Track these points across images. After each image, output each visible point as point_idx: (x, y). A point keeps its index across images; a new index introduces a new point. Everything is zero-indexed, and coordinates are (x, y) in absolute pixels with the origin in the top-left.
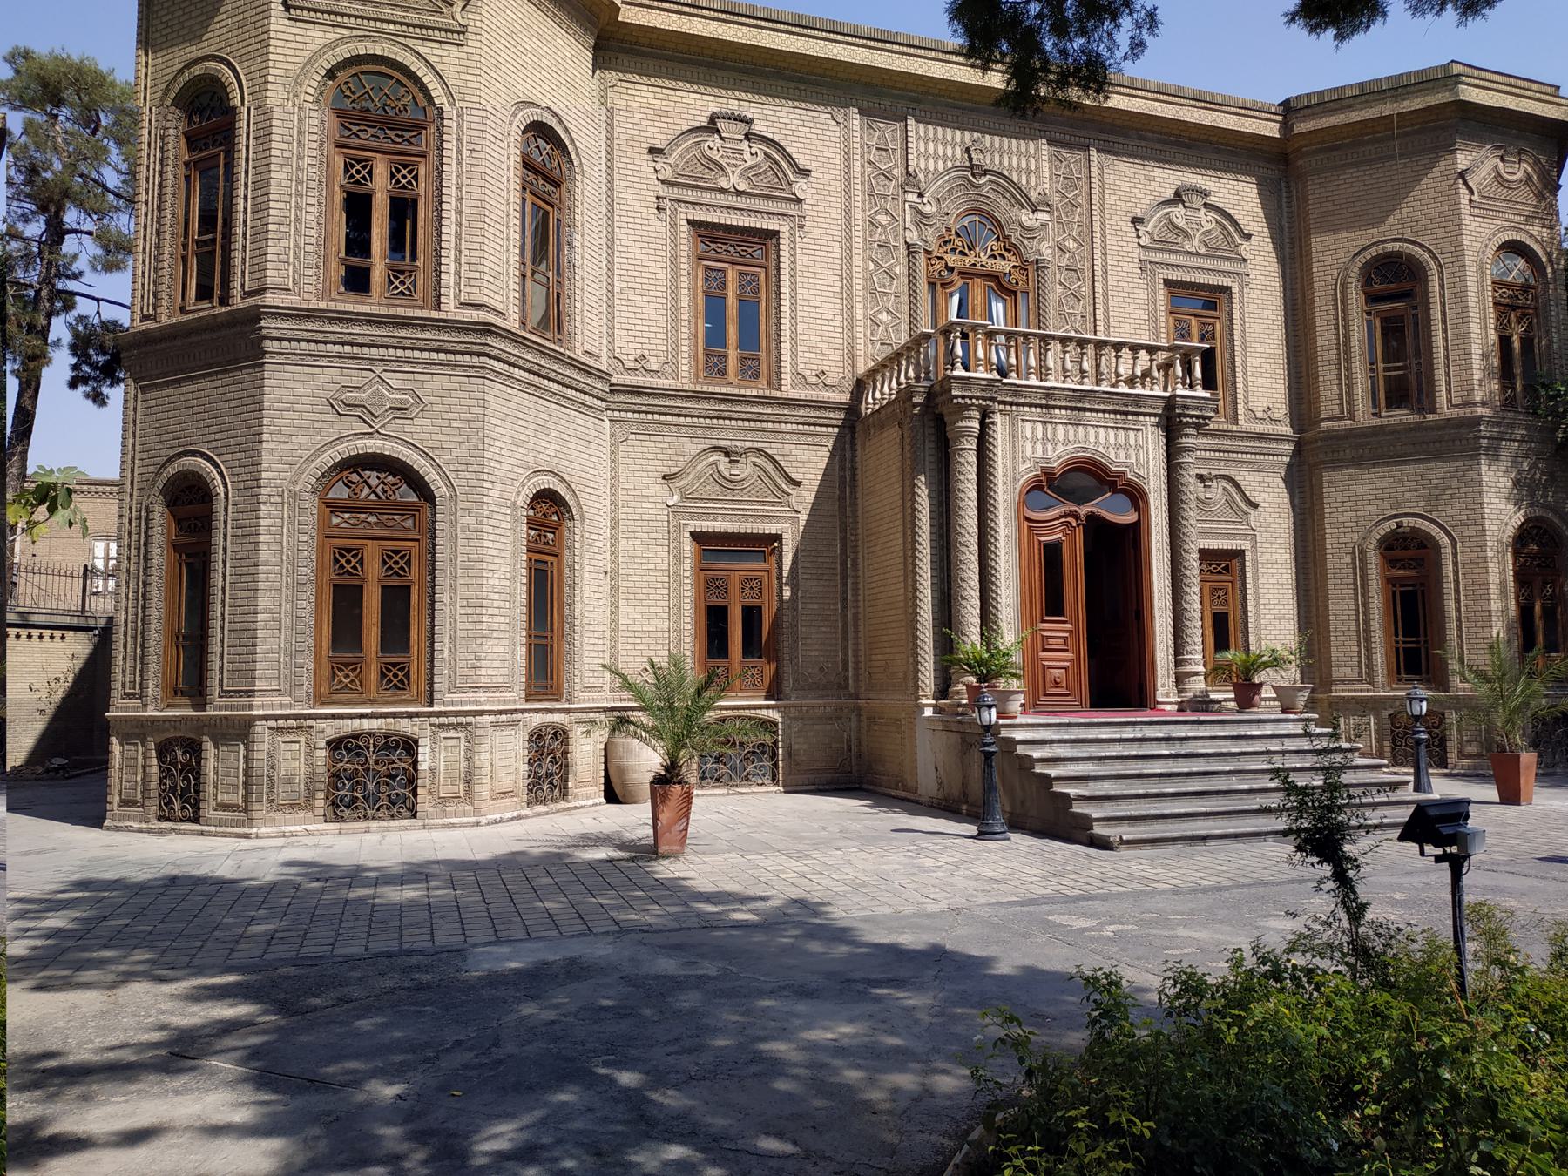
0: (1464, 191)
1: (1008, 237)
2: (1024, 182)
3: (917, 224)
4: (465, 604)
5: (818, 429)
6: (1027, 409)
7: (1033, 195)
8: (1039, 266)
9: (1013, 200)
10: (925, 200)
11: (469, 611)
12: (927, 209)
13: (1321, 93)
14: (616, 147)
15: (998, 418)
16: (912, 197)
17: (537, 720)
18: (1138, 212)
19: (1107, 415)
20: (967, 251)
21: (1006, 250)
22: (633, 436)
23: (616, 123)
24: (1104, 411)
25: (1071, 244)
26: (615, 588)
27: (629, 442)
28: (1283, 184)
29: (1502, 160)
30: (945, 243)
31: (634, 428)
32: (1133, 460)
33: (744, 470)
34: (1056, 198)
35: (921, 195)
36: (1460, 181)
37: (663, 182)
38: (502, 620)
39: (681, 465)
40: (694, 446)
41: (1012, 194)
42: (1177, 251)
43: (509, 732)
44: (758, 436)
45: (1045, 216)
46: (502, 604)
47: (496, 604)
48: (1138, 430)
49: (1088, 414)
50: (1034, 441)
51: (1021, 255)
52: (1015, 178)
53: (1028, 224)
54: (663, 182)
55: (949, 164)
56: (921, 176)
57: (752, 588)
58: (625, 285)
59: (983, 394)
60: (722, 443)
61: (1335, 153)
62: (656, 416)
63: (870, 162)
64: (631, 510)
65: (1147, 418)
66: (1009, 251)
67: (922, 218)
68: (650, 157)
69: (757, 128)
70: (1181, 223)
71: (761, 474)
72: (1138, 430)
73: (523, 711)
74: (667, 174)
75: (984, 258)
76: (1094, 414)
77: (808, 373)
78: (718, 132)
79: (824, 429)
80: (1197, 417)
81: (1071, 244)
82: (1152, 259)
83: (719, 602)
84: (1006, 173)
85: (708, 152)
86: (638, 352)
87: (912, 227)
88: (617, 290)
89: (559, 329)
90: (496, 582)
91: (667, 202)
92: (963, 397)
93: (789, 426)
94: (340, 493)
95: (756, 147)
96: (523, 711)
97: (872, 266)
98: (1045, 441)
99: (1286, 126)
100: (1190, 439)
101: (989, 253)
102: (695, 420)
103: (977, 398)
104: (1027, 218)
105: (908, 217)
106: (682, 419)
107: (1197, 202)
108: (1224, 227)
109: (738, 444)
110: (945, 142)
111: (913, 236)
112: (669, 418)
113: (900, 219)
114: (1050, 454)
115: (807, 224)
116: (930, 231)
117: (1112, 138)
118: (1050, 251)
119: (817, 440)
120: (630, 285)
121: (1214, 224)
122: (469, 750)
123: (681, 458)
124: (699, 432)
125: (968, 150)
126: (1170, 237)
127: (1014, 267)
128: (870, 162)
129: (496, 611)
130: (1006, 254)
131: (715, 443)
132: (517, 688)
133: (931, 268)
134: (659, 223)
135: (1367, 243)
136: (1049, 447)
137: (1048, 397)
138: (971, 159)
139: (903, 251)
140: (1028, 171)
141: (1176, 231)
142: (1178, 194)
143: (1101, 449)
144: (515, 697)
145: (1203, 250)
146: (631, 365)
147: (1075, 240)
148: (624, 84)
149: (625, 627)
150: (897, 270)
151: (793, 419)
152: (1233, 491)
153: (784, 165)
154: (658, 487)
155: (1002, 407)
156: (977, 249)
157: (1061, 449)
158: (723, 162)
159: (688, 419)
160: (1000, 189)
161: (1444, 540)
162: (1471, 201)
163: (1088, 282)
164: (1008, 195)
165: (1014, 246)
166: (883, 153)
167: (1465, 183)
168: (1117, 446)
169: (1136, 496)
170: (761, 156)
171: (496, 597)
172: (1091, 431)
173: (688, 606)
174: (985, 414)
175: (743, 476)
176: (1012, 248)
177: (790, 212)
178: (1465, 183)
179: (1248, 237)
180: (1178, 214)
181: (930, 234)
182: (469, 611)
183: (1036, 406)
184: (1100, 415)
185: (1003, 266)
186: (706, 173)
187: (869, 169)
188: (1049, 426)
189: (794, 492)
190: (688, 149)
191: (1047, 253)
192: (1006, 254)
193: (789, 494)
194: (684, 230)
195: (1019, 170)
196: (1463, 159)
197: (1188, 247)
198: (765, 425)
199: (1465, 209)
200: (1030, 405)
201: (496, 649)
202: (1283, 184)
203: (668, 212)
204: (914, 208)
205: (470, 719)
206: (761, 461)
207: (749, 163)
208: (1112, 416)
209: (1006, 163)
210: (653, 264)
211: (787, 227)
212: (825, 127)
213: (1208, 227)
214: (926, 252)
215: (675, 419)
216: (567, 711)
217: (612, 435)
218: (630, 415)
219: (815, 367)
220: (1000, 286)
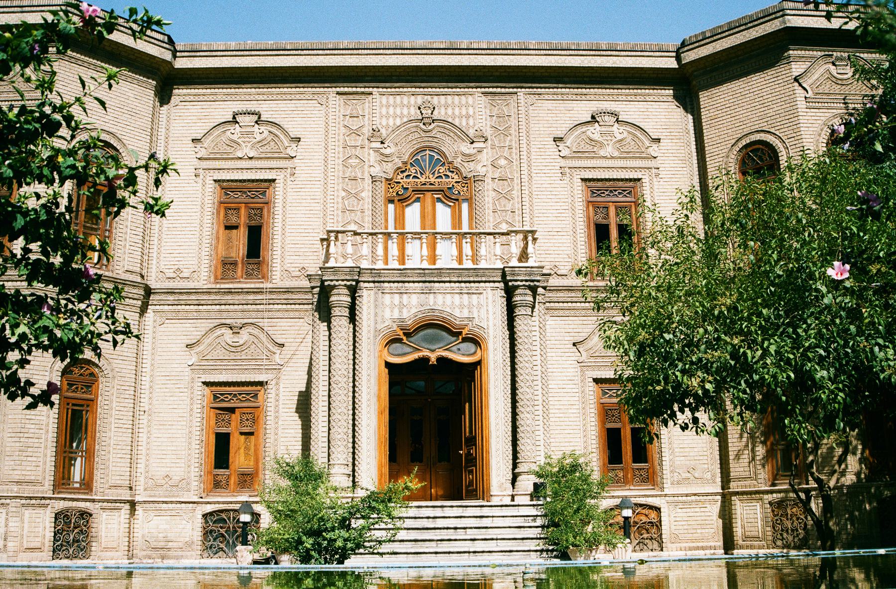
0: (800, 91)
1: (451, 163)
2: (464, 123)
3: (380, 162)
4: (10, 430)
5: (297, 306)
6: (386, 285)
7: (471, 133)
8: (477, 179)
9: (456, 138)
10: (385, 146)
11: (13, 435)
12: (387, 151)
13: (704, 33)
14: (170, 142)
15: (365, 293)
16: (378, 145)
17: (62, 505)
18: (560, 134)
19: (453, 284)
20: (419, 176)
21: (451, 171)
22: (167, 321)
23: (172, 128)
24: (450, 282)
25: (502, 162)
27: (165, 325)
28: (688, 100)
29: (834, 64)
30: (402, 172)
31: (169, 315)
32: (475, 315)
33: (244, 336)
34: (488, 132)
35: (382, 143)
36: (796, 84)
37: (199, 159)
38: (37, 440)
39: (198, 337)
40: (208, 325)
41: (454, 133)
42: (593, 158)
43: (41, 511)
44: (254, 314)
45: (481, 145)
46: (37, 431)
47: (32, 431)
48: (481, 293)
49: (437, 285)
50: (392, 307)
51: (461, 174)
52: (457, 122)
53: (467, 152)
54: (199, 159)
55: (405, 120)
56: (383, 131)
57: (247, 420)
58: (171, 226)
59: (348, 278)
60: (228, 321)
61: (714, 74)
62: (183, 307)
63: (345, 126)
64: (163, 370)
65: (487, 284)
66: (453, 172)
67: (385, 158)
68: (192, 145)
70: (596, 137)
71: (256, 341)
72: (481, 293)
73: (50, 498)
74: (203, 153)
75: (432, 180)
76: (442, 284)
77: (293, 269)
78: (237, 122)
79: (301, 306)
80: (526, 281)
81: (502, 162)
82: (571, 166)
83: (224, 430)
84: (450, 120)
85: (232, 137)
86: (176, 267)
87: (376, 165)
88: (165, 229)
90: (33, 417)
91: (201, 171)
92: (332, 280)
93: (276, 306)
95: (263, 128)
96: (50, 498)
97: (344, 194)
98: (402, 306)
99: (678, 58)
100: (522, 297)
101: (436, 175)
102: (209, 307)
103: (343, 280)
104: (466, 148)
105: (372, 159)
106: (200, 307)
107: (611, 120)
108: (634, 135)
109: (239, 321)
111: (376, 171)
112: (192, 307)
113: (366, 161)
114: (405, 315)
115: (296, 172)
116: (390, 164)
117: (534, 85)
118: (484, 169)
119: (297, 314)
120: (174, 225)
121: (626, 134)
122: (7, 519)
123: (199, 333)
124: (213, 315)
125: (419, 108)
126: (590, 149)
127: (456, 182)
128: (345, 126)
129: (31, 435)
130: (450, 174)
131: (223, 321)
132: (47, 484)
133: (391, 190)
134: (195, 184)
135: (739, 136)
136: (405, 310)
137: (401, 275)
138: (422, 114)
139: (368, 181)
140: (468, 117)
141: (593, 143)
142: (593, 117)
143: (448, 310)
144: (46, 489)
145: (616, 154)
146: (172, 275)
147: (506, 158)
148: (183, 104)
149: (155, 448)
150: (363, 194)
151: (278, 302)
153: (282, 137)
154: (183, 353)
155: (366, 285)
156: (427, 173)
157: (414, 310)
158: (239, 141)
159: (205, 307)
160: (446, 131)
162: (806, 98)
163: (517, 188)
164: (452, 134)
165: (457, 168)
166: (355, 119)
167: (800, 85)
168: (462, 306)
170: (266, 133)
171: (33, 426)
172: (440, 297)
173: (196, 433)
174: (353, 291)
175: (241, 342)
177: (285, 166)
178: (800, 85)
179: (658, 140)
180: (594, 131)
181: (390, 168)
182: (13, 435)
183: (394, 282)
184: (447, 285)
186: (229, 149)
187: (343, 130)
188: (405, 296)
189: (278, 352)
190: (219, 136)
191: (482, 171)
192: (450, 174)
193: (274, 353)
194: (210, 186)
195: (461, 117)
196: (797, 68)
197: (602, 153)
198: (258, 307)
199: (802, 104)
200: (389, 282)
201: (29, 459)
202: (688, 100)
203: (201, 177)
204: (376, 150)
205: (8, 501)
206: (256, 332)
207: (258, 139)
208: (457, 284)
209: (450, 111)
210: (190, 210)
211: (282, 176)
212: (312, 109)
213: (619, 137)
214: (387, 180)
215: (196, 307)
216: (93, 501)
217: (155, 321)
218: (166, 307)
219: (298, 265)
220: (448, 196)
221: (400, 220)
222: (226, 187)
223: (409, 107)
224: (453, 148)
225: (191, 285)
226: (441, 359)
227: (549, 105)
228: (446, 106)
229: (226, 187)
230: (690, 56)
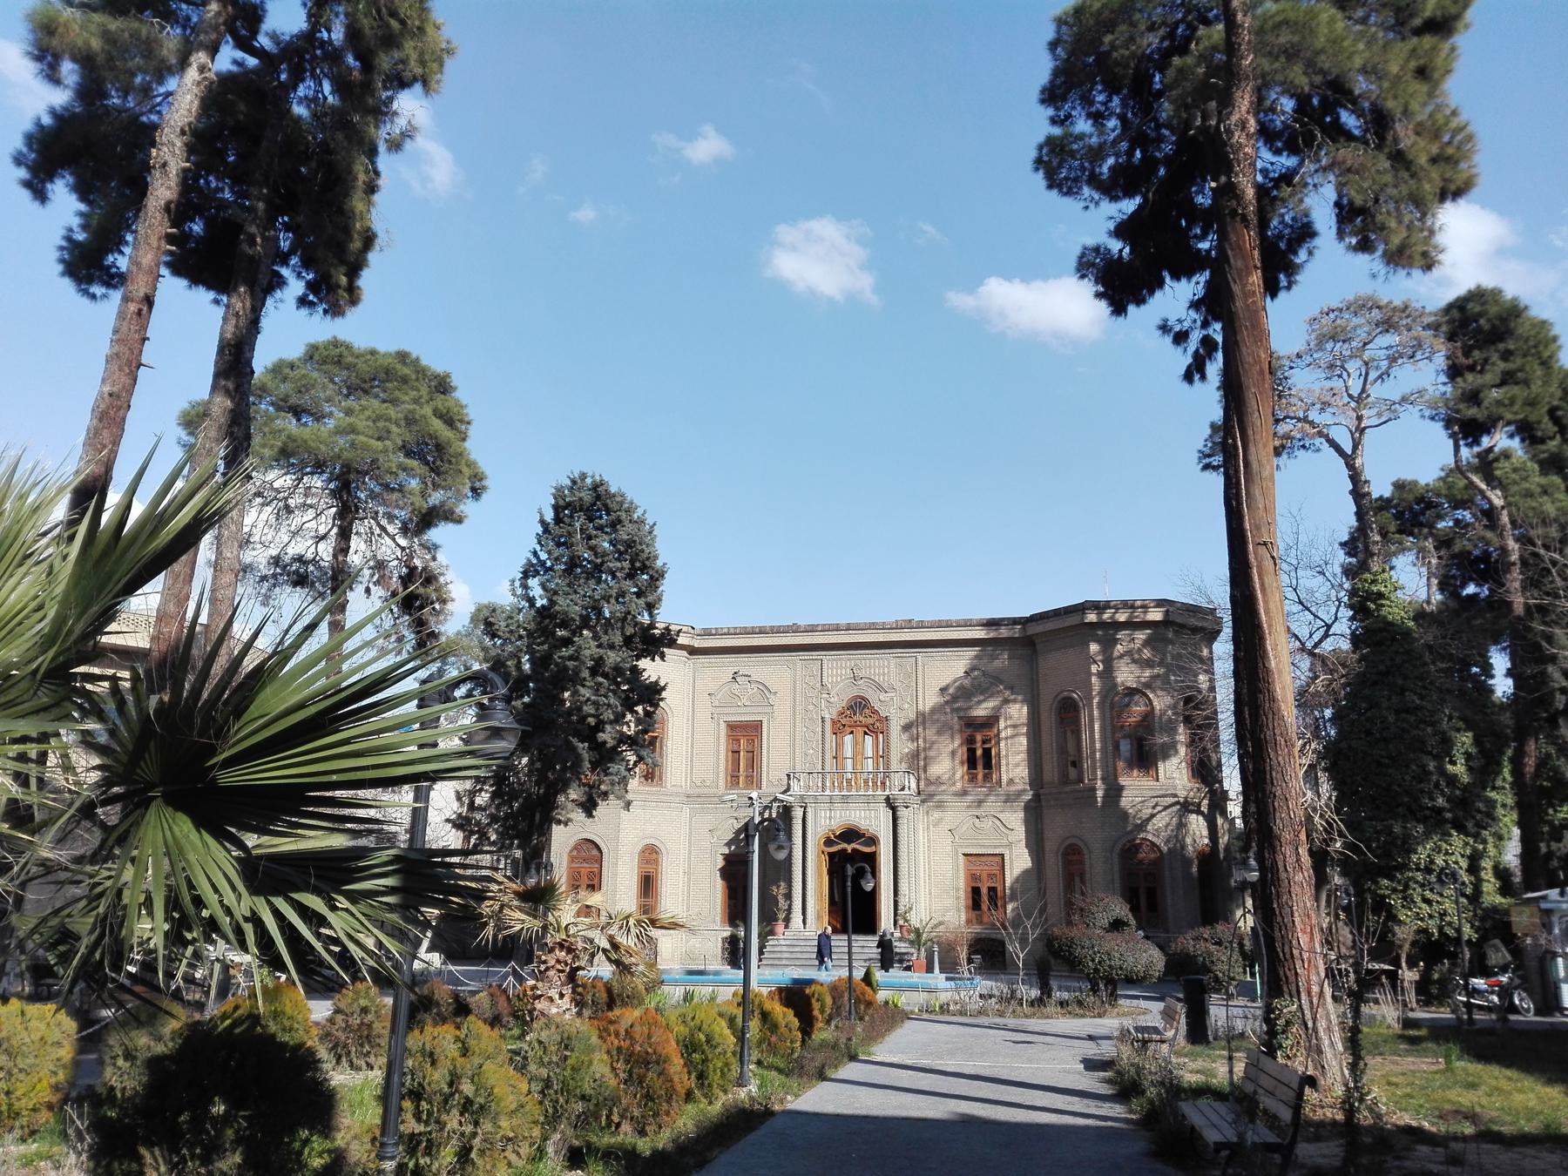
7: (885, 685)
15: (809, 810)
25: (906, 706)
26: (689, 879)
34: (897, 685)
69: (753, 678)
81: (906, 706)
89: (661, 779)
94: (575, 853)
98: (830, 818)
110: (841, 668)
140: (884, 674)
152: (998, 822)
161: (1085, 851)
168: (865, 818)
169: (873, 841)
176: (875, 712)
185: (870, 721)
194: (723, 726)
220: (870, 730)
221: (839, 746)
222: (733, 727)
223: (846, 668)
224: (875, 698)
225: (712, 791)
226: (853, 850)
227: (937, 663)
228: (870, 667)
229: (733, 727)
230: (1033, 629)
